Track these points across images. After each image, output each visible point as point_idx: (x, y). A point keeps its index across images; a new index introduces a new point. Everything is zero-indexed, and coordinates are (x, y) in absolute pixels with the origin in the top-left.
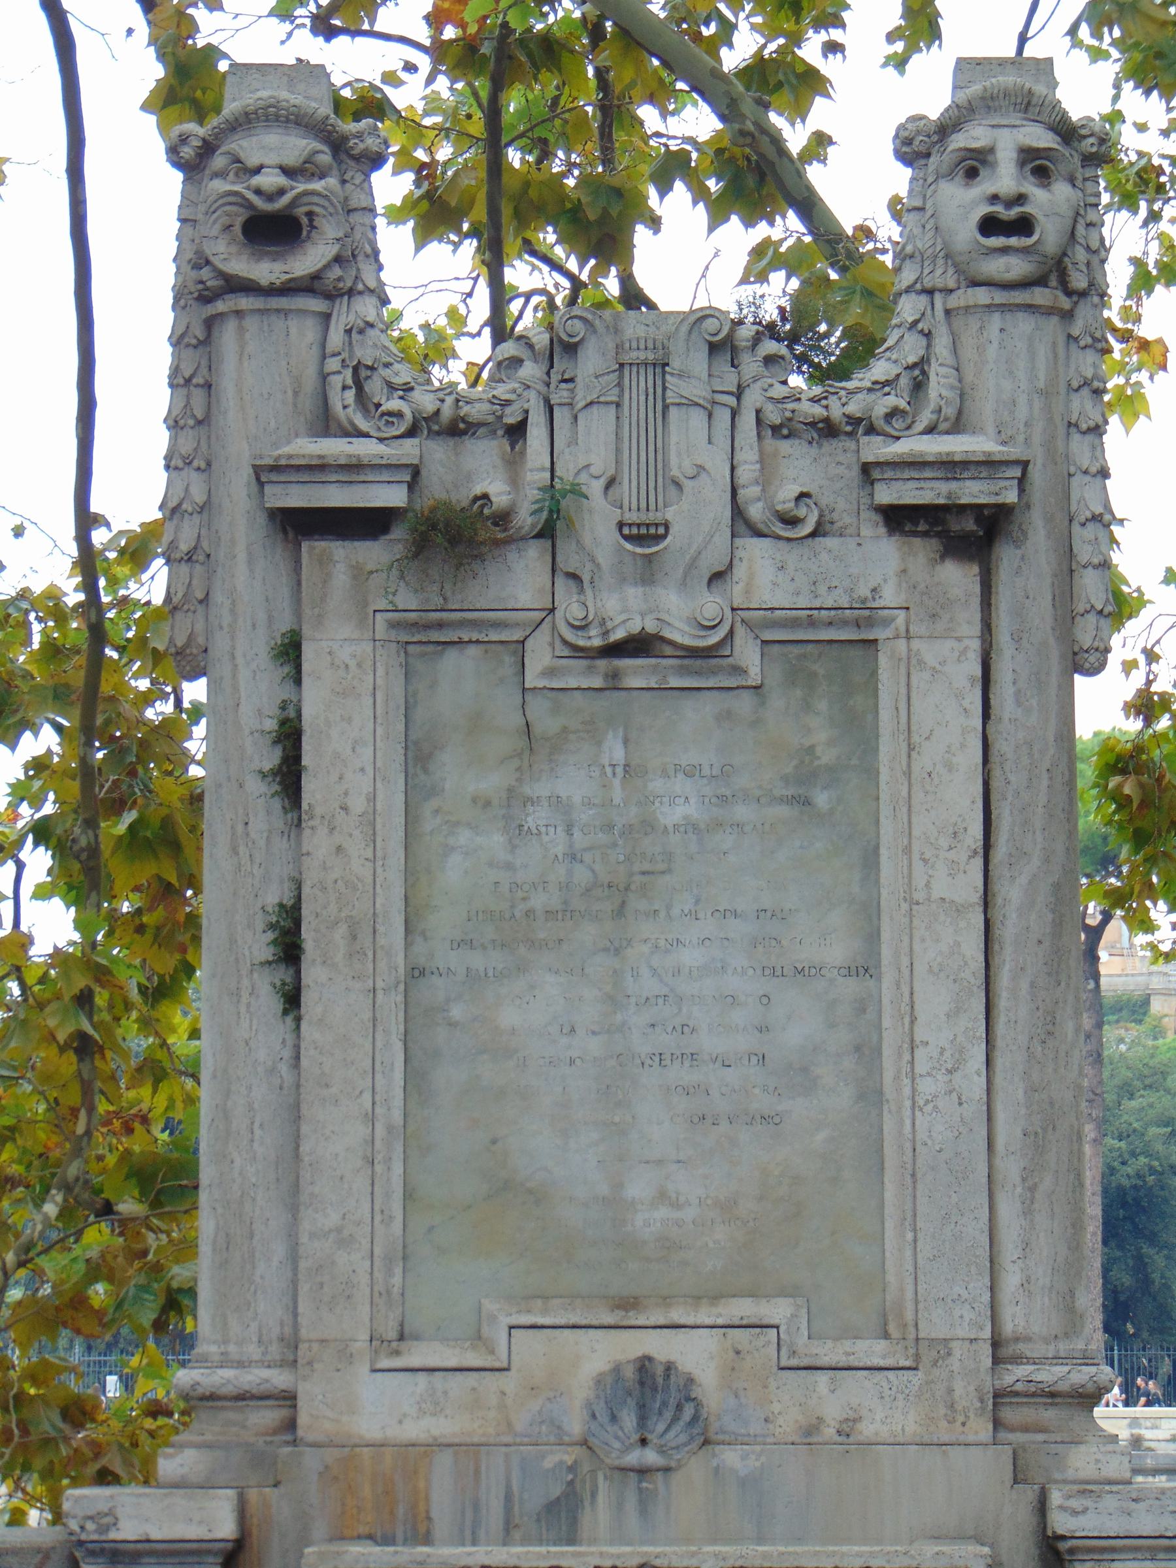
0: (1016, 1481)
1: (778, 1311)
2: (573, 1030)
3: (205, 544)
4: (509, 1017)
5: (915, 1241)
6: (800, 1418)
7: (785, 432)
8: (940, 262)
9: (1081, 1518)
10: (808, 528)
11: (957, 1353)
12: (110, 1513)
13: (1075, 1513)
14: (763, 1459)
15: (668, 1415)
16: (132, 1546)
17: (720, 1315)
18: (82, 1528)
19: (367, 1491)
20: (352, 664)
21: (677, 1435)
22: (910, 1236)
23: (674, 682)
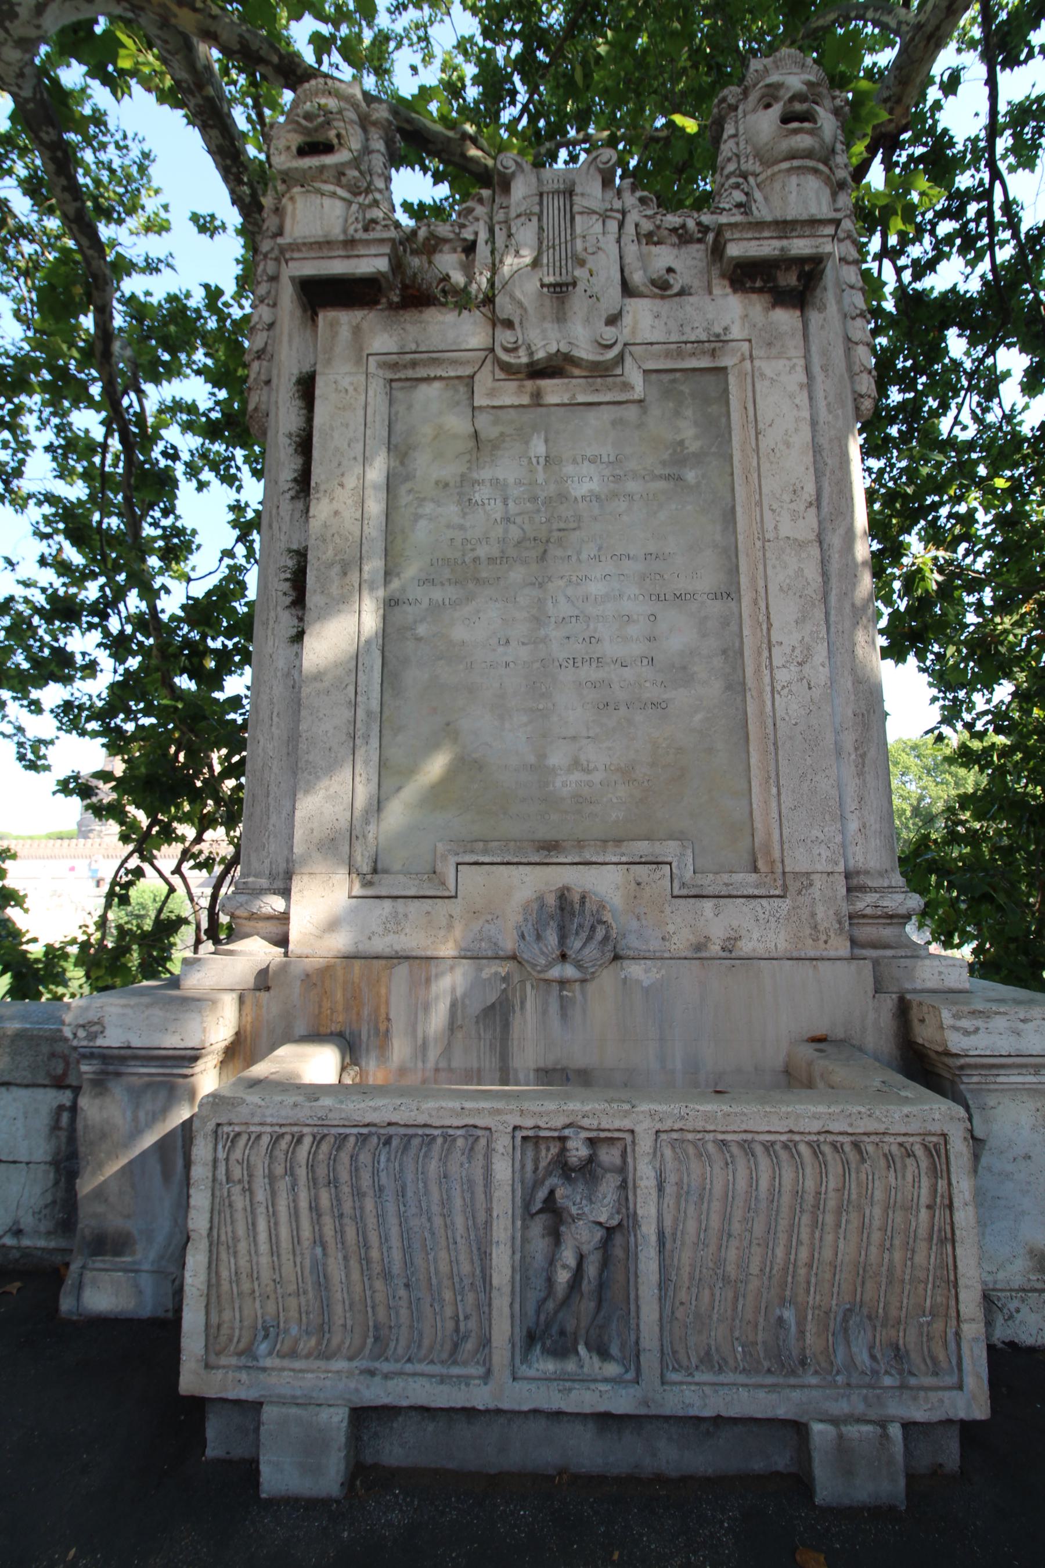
0: (877, 991)
1: (669, 850)
2: (508, 642)
3: (269, 348)
4: (459, 633)
5: (779, 794)
6: (691, 937)
7: (655, 239)
8: (751, 158)
9: (972, 1037)
10: (676, 289)
11: (818, 884)
12: (99, 1022)
13: (967, 1033)
14: (663, 972)
15: (584, 935)
16: (116, 1052)
17: (623, 854)
18: (75, 1035)
19: (339, 995)
20: (351, 389)
21: (591, 952)
22: (774, 790)
23: (581, 399)
